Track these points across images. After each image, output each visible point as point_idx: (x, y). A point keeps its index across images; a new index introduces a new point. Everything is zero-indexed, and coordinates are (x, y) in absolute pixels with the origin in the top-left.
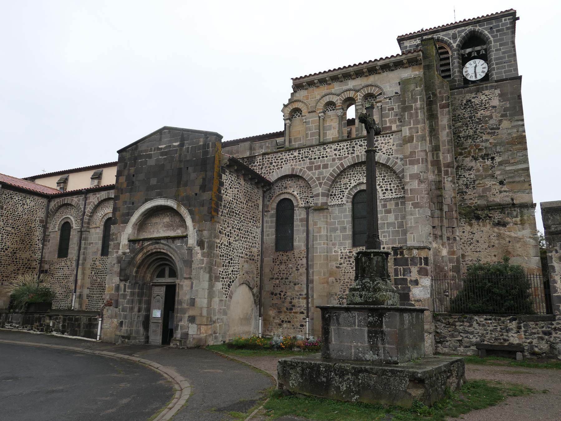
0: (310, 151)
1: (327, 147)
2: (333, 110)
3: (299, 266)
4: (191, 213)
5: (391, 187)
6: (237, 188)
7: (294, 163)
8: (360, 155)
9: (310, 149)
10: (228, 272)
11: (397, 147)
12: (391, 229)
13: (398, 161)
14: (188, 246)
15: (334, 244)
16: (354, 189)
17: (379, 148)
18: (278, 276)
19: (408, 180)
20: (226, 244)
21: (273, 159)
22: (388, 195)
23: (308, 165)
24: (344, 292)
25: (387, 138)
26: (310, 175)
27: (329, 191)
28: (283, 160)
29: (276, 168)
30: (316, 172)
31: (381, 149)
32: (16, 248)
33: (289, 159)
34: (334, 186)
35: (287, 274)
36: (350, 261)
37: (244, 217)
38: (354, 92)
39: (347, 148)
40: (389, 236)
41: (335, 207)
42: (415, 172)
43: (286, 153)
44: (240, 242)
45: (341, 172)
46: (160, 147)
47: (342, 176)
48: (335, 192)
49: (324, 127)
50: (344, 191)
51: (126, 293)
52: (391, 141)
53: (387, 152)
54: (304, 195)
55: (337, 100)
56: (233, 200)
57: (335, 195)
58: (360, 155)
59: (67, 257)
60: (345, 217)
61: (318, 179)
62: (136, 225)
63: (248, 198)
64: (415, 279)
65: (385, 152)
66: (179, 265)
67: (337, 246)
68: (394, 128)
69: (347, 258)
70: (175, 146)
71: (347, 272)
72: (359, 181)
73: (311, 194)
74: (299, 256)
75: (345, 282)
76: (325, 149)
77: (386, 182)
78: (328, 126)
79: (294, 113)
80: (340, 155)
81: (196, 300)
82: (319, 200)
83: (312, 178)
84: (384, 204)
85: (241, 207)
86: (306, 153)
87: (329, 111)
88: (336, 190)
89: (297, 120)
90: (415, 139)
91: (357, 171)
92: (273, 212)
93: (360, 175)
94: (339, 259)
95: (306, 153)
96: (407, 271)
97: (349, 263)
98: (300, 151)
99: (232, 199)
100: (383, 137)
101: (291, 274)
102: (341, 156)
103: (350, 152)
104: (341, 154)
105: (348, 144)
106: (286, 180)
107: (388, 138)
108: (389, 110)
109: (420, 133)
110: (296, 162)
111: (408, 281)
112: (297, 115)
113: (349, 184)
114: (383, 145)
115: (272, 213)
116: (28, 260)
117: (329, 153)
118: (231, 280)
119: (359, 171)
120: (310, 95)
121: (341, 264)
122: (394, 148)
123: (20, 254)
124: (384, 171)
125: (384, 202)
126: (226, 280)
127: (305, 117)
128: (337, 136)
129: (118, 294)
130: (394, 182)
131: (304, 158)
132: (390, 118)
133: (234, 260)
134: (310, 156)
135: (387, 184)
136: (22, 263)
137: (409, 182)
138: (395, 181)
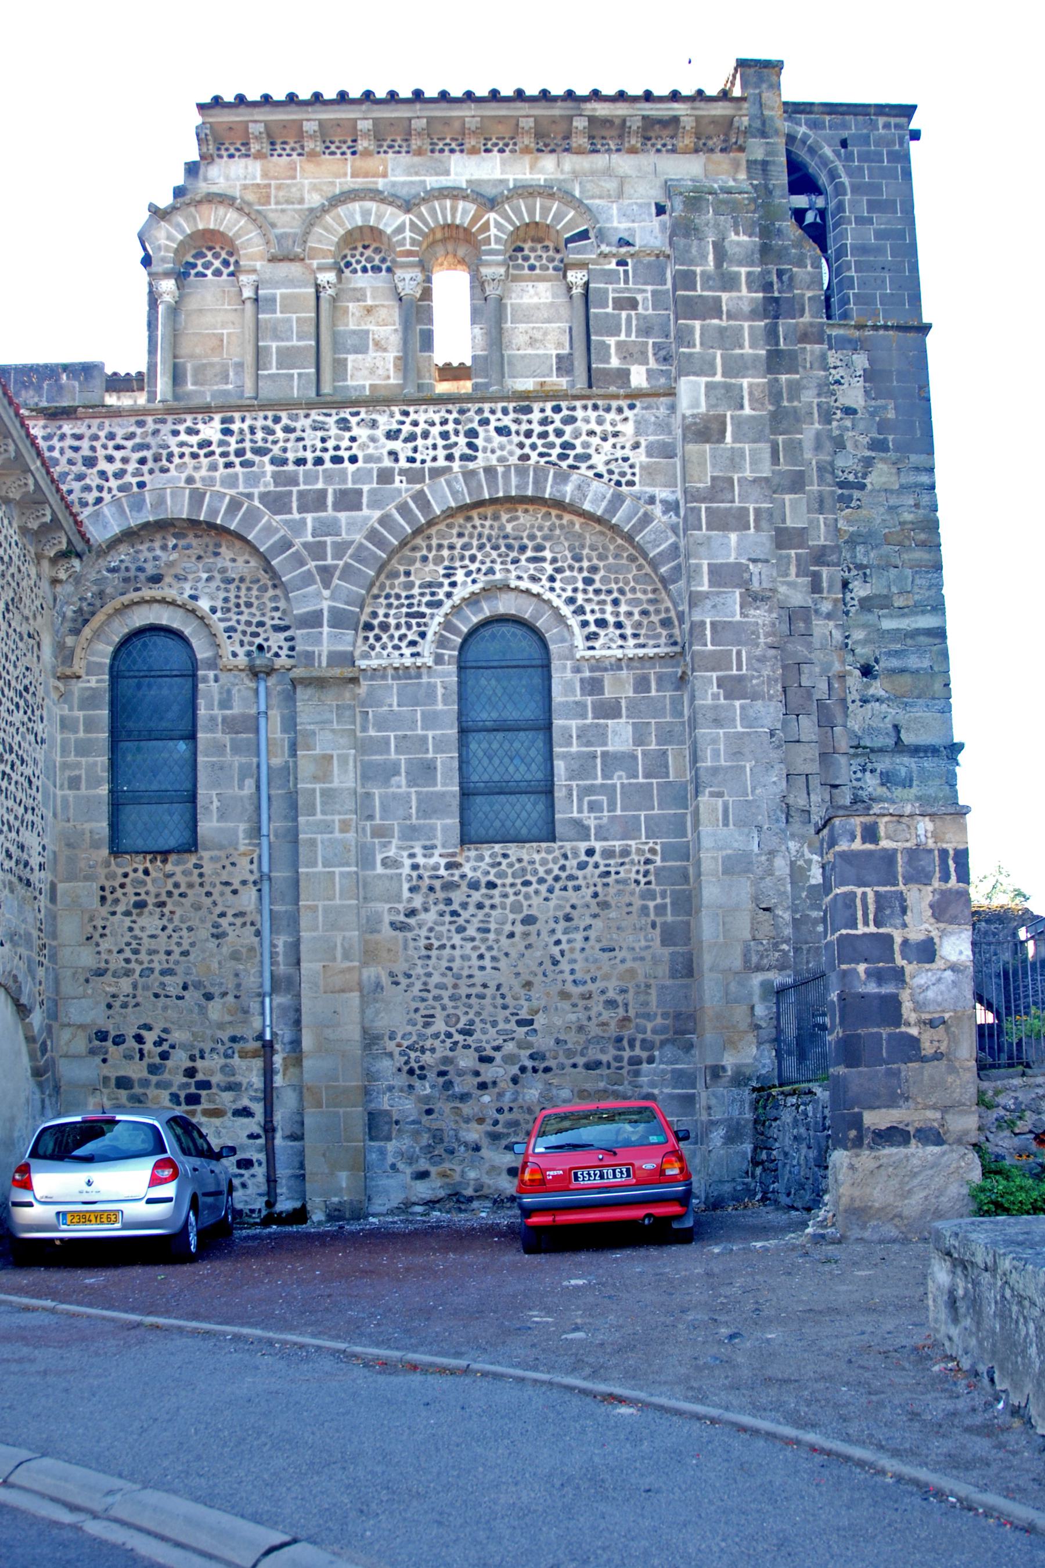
0: (278, 428)
1: (354, 420)
5: (617, 614)
7: (203, 472)
8: (500, 470)
11: (649, 454)
12: (619, 779)
13: (657, 510)
15: (380, 832)
16: (467, 611)
17: (579, 450)
18: (127, 961)
23: (266, 485)
28: (148, 454)
29: (113, 483)
30: (303, 521)
31: (588, 457)
33: (176, 451)
36: (449, 902)
38: (472, 208)
39: (445, 435)
40: (612, 807)
41: (384, 677)
42: (732, 560)
43: (164, 421)
47: (414, 549)
48: (386, 615)
49: (335, 335)
50: (423, 615)
52: (628, 429)
53: (611, 472)
54: (243, 618)
57: (385, 627)
61: (317, 550)
64: (922, 937)
65: (602, 469)
67: (395, 842)
68: (638, 378)
71: (436, 944)
72: (490, 577)
73: (277, 614)
74: (224, 879)
76: (344, 425)
77: (597, 592)
78: (354, 332)
79: (195, 256)
80: (412, 460)
83: (288, 545)
84: (592, 679)
86: (260, 435)
87: (355, 271)
88: (389, 606)
91: (480, 536)
93: (494, 554)
94: (406, 894)
95: (260, 435)
97: (448, 909)
100: (595, 407)
102: (417, 465)
103: (457, 452)
104: (419, 457)
105: (451, 417)
106: (157, 544)
110: (213, 467)
111: (897, 948)
113: (446, 588)
114: (595, 441)
119: (489, 539)
120: (279, 187)
121: (412, 913)
124: (593, 548)
125: (592, 670)
127: (254, 277)
130: (629, 596)
131: (249, 455)
132: (623, 337)
134: (276, 450)
135: (604, 602)
137: (706, 595)
138: (633, 590)
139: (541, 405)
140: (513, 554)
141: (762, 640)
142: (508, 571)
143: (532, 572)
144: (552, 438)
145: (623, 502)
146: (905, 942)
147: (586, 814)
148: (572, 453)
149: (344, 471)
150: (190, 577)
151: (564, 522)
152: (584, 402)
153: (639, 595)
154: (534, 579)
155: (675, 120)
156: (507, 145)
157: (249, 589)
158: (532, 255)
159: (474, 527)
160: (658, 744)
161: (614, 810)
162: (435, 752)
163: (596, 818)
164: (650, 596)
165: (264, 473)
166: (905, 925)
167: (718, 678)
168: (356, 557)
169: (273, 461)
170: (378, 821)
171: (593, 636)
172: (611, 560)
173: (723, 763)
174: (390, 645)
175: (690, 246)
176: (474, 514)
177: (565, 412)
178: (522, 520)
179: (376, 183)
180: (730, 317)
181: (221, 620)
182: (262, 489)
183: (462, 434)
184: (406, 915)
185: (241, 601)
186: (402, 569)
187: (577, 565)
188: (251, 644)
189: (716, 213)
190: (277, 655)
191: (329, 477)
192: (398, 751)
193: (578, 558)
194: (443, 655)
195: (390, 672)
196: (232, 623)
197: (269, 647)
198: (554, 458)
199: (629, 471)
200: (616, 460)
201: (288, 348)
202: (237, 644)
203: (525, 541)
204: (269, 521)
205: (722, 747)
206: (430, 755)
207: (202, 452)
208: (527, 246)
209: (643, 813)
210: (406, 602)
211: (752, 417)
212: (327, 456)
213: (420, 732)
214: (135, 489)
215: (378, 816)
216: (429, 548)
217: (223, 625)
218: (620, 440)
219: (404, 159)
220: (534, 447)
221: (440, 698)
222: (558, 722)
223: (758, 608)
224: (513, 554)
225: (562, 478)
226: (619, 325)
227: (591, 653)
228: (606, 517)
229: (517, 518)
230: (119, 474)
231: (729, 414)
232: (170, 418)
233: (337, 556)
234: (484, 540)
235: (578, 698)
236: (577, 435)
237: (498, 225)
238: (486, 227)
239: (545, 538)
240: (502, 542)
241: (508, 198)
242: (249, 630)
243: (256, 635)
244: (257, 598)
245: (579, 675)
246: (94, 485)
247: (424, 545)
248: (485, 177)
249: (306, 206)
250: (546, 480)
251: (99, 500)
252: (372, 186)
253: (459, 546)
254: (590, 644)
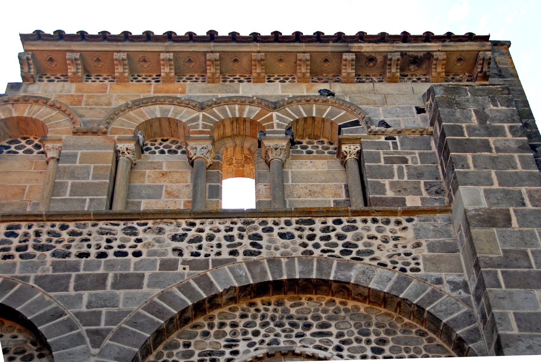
1: (140, 229)
65: (384, 260)
91: (263, 317)
93: (278, 330)
119: (273, 318)
159: (258, 310)
165: (44, 263)
178: (306, 305)
182: (39, 273)
187: (364, 338)
191: (111, 266)
216: (211, 326)
239: (330, 318)
240: (286, 321)
247: (206, 323)
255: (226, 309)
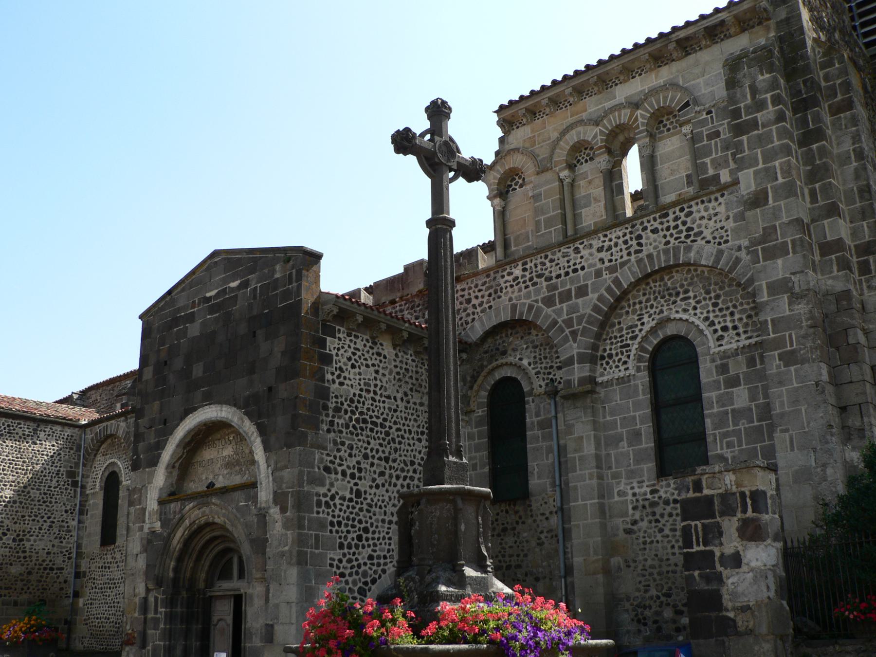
0: (547, 261)
1: (581, 247)
2: (592, 159)
3: (543, 536)
4: (262, 431)
5: (734, 321)
6: (373, 365)
8: (655, 254)
9: (546, 257)
10: (357, 560)
11: (735, 221)
12: (743, 425)
13: (743, 254)
14: (259, 505)
16: (651, 338)
17: (696, 230)
19: (764, 297)
20: (348, 496)
21: (471, 291)
22: (731, 344)
24: (646, 591)
25: (710, 205)
26: (550, 316)
27: (595, 348)
28: (492, 291)
30: (562, 308)
31: (701, 232)
32: (24, 531)
33: (503, 285)
34: (608, 334)
35: (518, 556)
36: (654, 514)
37: (398, 430)
38: (628, 111)
39: (626, 242)
40: (740, 444)
41: (612, 385)
42: (780, 277)
43: (498, 272)
44: (391, 488)
45: (619, 300)
46: (208, 295)
47: (622, 308)
48: (611, 349)
50: (628, 345)
51: (159, 616)
52: (722, 209)
53: (715, 238)
54: (543, 366)
55: (595, 137)
56: (364, 394)
57: (610, 356)
58: (655, 254)
59: (114, 543)
60: (637, 406)
61: (569, 323)
62: (174, 467)
63: (410, 386)
64: (732, 551)
65: (709, 238)
66: (246, 549)
67: (623, 480)
68: (725, 177)
69: (647, 506)
70: (232, 290)
71: (648, 540)
72: (661, 315)
73: (558, 360)
74: (542, 511)
75: (647, 568)
76: (577, 250)
78: (584, 196)
79: (511, 181)
80: (610, 261)
81: (276, 627)
82: (573, 374)
83: (555, 322)
84: (722, 364)
85: (390, 409)
86: (539, 267)
87: (582, 164)
88: (612, 344)
89: (518, 197)
90: (770, 194)
91: (654, 292)
92: (481, 412)
93: (662, 301)
94: (631, 511)
96: (714, 533)
98: (525, 264)
99: (358, 392)
100: (703, 202)
101: (526, 555)
102: (614, 263)
103: (632, 250)
105: (627, 231)
106: (504, 335)
107: (713, 204)
108: (710, 137)
109: (781, 180)
110: (520, 290)
111: (716, 559)
112: (516, 184)
115: (480, 414)
116: (48, 553)
117: (586, 260)
118: (369, 579)
119: (659, 293)
120: (539, 135)
121: (635, 522)
122: (730, 224)
123: (32, 543)
124: (716, 284)
125: (721, 359)
126: (350, 579)
128: (604, 217)
129: (145, 619)
131: (535, 279)
132: (714, 156)
133: (374, 533)
134: (547, 273)
135: (725, 315)
136: (37, 560)
137: (767, 303)
138: (741, 304)
139: (673, 210)
140: (673, 299)
141: (804, 324)
142: (671, 309)
143: (684, 307)
144: (681, 227)
145: (723, 254)
146: (722, 555)
147: (725, 450)
148: (692, 233)
149: (579, 276)
150: (519, 348)
151: (699, 272)
152: (696, 201)
153: (745, 306)
154: (685, 311)
155: (722, 23)
156: (642, 70)
157: (545, 349)
158: (668, 123)
160: (764, 399)
161: (741, 445)
162: (640, 425)
163: (731, 452)
164: (752, 305)
165: (542, 287)
166: (721, 544)
167: (779, 355)
168: (588, 322)
169: (546, 280)
170: (614, 470)
171: (721, 338)
172: (727, 289)
173: (787, 409)
174: (614, 366)
175: (736, 93)
176: (650, 280)
177: (687, 210)
179: (582, 116)
180: (764, 126)
181: (533, 369)
182: (542, 296)
183: (634, 239)
184: (632, 524)
185: (542, 357)
186: (616, 321)
187: (708, 297)
188: (548, 379)
189: (749, 67)
190: (560, 383)
191: (572, 281)
192: (622, 427)
193: (708, 292)
194: (640, 366)
195: (615, 381)
196: (539, 369)
197: (556, 379)
198: (683, 239)
199: (725, 234)
200: (717, 230)
201: (548, 218)
202: (541, 380)
203: (679, 289)
204: (546, 312)
205: (785, 399)
206: (638, 427)
207: (514, 284)
208: (664, 119)
209: (758, 445)
210: (619, 340)
211: (784, 183)
212: (570, 270)
213: (632, 414)
214: (488, 310)
215: (614, 467)
216: (629, 306)
217: (534, 371)
218: (718, 218)
219: (594, 98)
220: (672, 235)
221: (641, 392)
222: (705, 395)
223: (799, 304)
224: (673, 299)
225: (688, 249)
226: (711, 149)
227: (722, 348)
228: (715, 266)
229: (673, 277)
230: (481, 305)
231: (769, 186)
232: (500, 270)
233: (579, 324)
234: (657, 295)
235: (715, 378)
236: (694, 222)
237: (642, 116)
238: (636, 119)
239: (689, 285)
241: (645, 100)
242: (546, 371)
243: (549, 373)
244: (549, 353)
245: (714, 364)
246: (471, 312)
247: (626, 305)
248: (633, 92)
249: (552, 140)
250: (680, 253)
251: (473, 320)
252: (580, 119)
253: (644, 301)
254: (720, 343)
255: (635, 292)
